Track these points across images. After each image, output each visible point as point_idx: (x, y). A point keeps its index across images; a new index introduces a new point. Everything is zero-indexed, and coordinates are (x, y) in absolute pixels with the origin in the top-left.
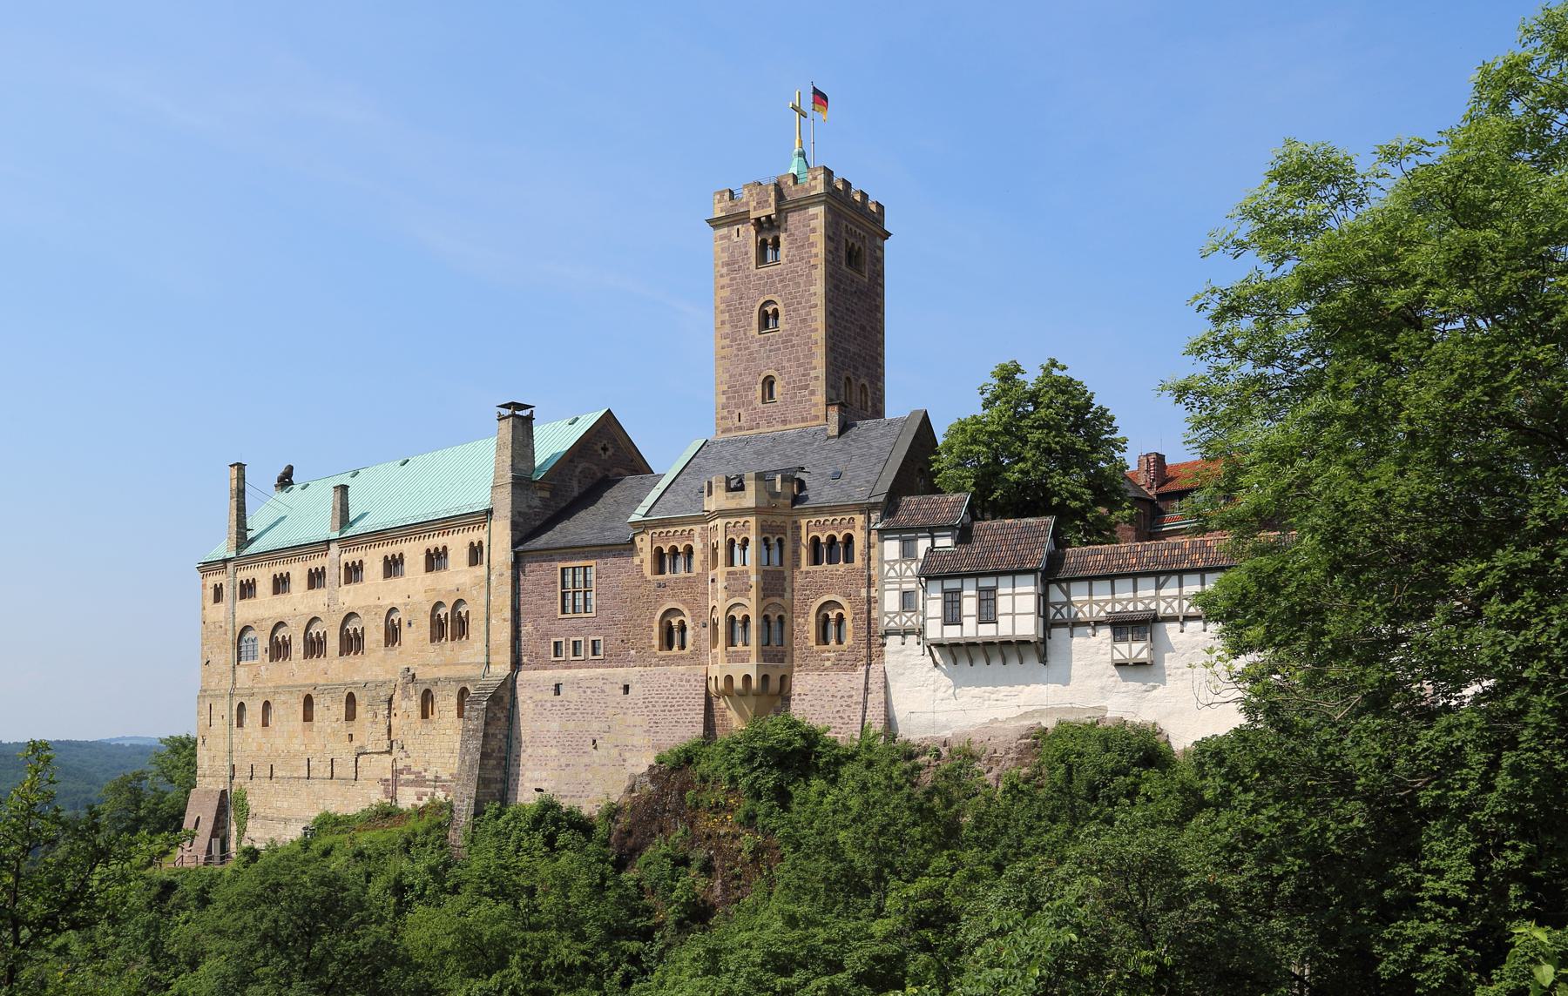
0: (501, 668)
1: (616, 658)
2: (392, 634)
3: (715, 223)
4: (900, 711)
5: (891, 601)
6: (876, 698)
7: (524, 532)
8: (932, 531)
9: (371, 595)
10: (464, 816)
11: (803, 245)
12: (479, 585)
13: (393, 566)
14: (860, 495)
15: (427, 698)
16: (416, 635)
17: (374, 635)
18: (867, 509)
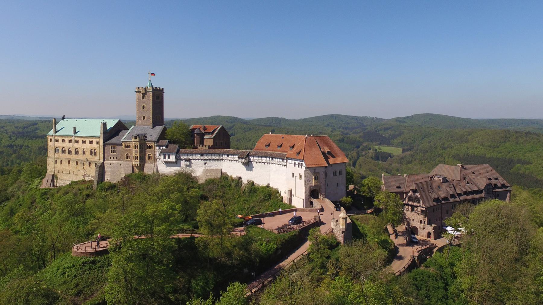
0: (102, 161)
1: (119, 160)
2: (84, 153)
3: (136, 92)
4: (159, 169)
5: (157, 155)
6: (156, 168)
7: (105, 140)
8: (163, 146)
9: (80, 146)
10: (96, 182)
11: (149, 97)
12: (99, 146)
13: (84, 142)
14: (154, 140)
15: (90, 164)
16: (88, 153)
17: (81, 152)
18: (154, 142)
